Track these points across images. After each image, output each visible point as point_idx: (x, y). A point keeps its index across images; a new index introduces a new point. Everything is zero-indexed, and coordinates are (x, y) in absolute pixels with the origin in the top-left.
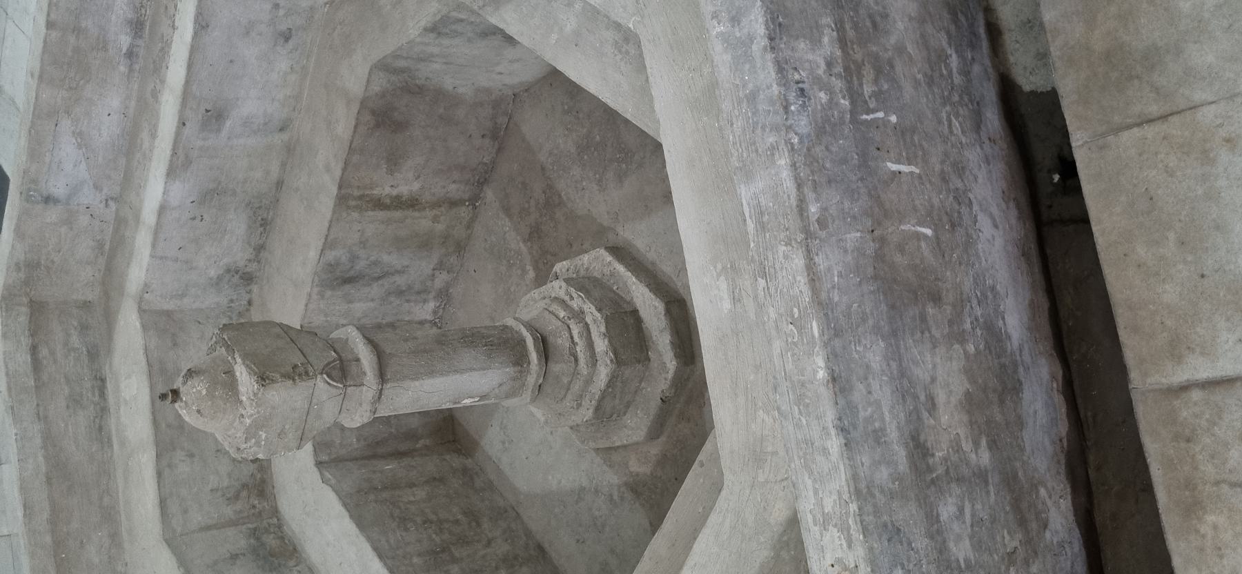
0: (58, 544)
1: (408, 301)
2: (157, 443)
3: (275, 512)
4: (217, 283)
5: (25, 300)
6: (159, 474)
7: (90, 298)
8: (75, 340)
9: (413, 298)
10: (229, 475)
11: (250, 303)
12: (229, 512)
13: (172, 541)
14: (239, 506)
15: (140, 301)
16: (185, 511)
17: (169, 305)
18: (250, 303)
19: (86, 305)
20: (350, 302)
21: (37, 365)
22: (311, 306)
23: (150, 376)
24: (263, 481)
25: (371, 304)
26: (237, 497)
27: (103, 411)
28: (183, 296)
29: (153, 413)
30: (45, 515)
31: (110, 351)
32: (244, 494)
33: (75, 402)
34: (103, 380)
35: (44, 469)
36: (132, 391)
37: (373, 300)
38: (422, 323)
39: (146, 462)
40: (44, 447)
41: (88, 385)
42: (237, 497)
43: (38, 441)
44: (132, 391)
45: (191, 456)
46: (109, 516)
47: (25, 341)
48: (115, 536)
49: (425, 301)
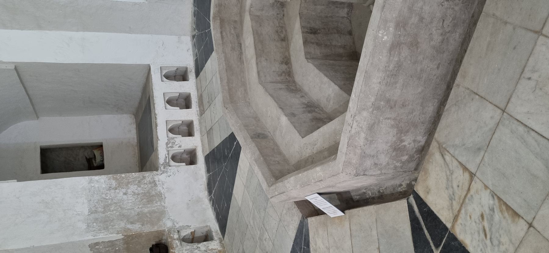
0: (230, 90)
1: (337, 7)
2: (256, 54)
3: (294, 82)
4: (273, 5)
5: (219, 18)
6: (257, 64)
7: (236, 19)
8: (233, 31)
9: (338, 6)
10: (279, 68)
11: (284, 15)
12: (279, 79)
13: (261, 83)
14: (282, 78)
15: (250, 11)
16: (265, 76)
17: (258, 13)
18: (284, 15)
19: (235, 22)
20: (315, 5)
21: (222, 37)
22: (302, 5)
23: (253, 34)
24: (290, 72)
25: (323, 7)
26: (281, 75)
27: (241, 53)
28: (262, 10)
29: (255, 46)
30: (226, 81)
31: (242, 34)
32: (284, 74)
33: (233, 49)
34: (241, 44)
35: (225, 67)
36: (249, 40)
37: (324, 5)
38: (343, 17)
39: (253, 62)
40: (225, 61)
41: (237, 45)
42: (281, 75)
43: (223, 59)
44: (249, 40)
45: (267, 60)
46: (244, 84)
47: (219, 30)
48: (245, 90)
49: (343, 8)
